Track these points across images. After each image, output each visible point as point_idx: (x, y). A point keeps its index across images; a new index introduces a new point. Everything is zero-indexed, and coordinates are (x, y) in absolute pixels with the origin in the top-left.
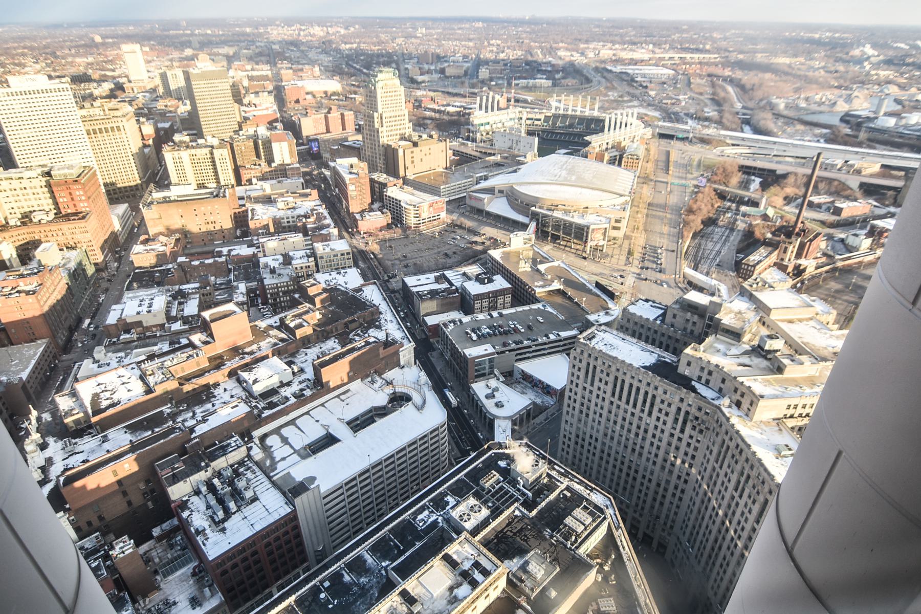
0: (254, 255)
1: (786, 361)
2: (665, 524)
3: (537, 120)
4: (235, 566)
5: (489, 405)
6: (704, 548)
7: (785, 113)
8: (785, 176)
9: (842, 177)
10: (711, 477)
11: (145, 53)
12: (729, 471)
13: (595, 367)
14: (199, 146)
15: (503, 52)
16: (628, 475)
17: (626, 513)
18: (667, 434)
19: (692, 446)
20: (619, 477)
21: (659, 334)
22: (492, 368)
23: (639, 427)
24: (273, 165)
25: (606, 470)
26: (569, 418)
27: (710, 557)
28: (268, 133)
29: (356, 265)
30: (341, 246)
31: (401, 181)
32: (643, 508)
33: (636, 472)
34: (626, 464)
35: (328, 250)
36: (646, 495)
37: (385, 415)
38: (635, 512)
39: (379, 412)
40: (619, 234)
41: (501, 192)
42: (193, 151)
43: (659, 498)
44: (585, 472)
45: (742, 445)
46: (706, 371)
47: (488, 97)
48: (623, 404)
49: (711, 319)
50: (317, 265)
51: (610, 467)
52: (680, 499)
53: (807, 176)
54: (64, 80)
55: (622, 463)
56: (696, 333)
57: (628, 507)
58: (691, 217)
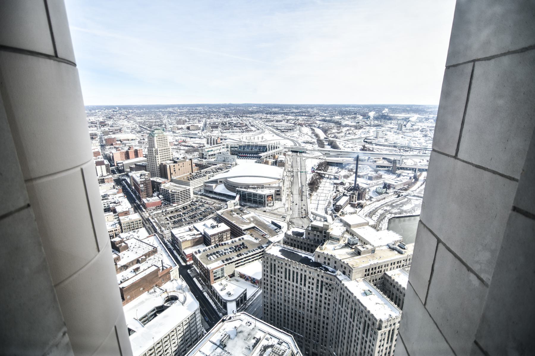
12: (346, 309)
16: (299, 320)
17: (302, 343)
18: (314, 294)
19: (327, 299)
23: (301, 293)
25: (288, 320)
29: (144, 226)
30: (135, 217)
33: (303, 318)
34: (298, 315)
35: (127, 220)
39: (161, 309)
41: (221, 182)
44: (278, 323)
50: (121, 228)
52: (327, 329)
55: (296, 315)
57: (302, 338)
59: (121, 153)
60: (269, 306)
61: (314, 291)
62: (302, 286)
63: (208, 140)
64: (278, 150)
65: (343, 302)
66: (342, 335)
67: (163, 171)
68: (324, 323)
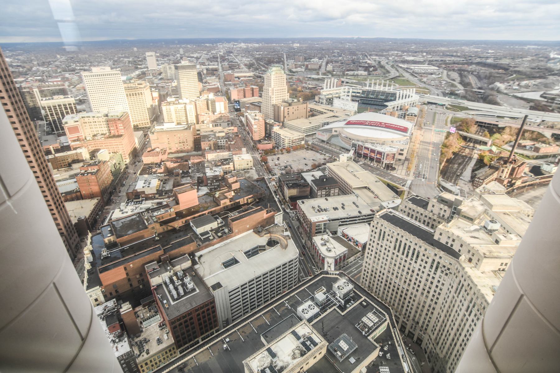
1: (501, 237)
2: (422, 327)
3: (358, 93)
4: (181, 324)
6: (446, 343)
7: (505, 91)
8: (503, 128)
9: (540, 130)
10: (451, 302)
11: (157, 57)
12: (463, 300)
13: (385, 232)
14: (179, 103)
15: (340, 56)
17: (399, 318)
20: (396, 297)
21: (424, 215)
22: (325, 228)
23: (409, 269)
24: (215, 114)
25: (388, 292)
26: (368, 260)
27: (449, 349)
28: (214, 98)
31: (281, 124)
32: (409, 316)
34: (400, 290)
36: (411, 309)
37: (264, 250)
38: (404, 318)
40: (403, 158)
42: (176, 106)
43: (419, 311)
44: (376, 292)
45: (471, 285)
46: (451, 239)
48: (400, 254)
49: (455, 209)
50: (234, 167)
51: (391, 291)
53: (518, 129)
54: (118, 69)
55: (398, 289)
56: (446, 217)
58: (446, 149)
60: (370, 273)
61: (426, 271)
62: (413, 262)
63: (327, 83)
65: (460, 291)
66: (450, 325)
67: (276, 113)
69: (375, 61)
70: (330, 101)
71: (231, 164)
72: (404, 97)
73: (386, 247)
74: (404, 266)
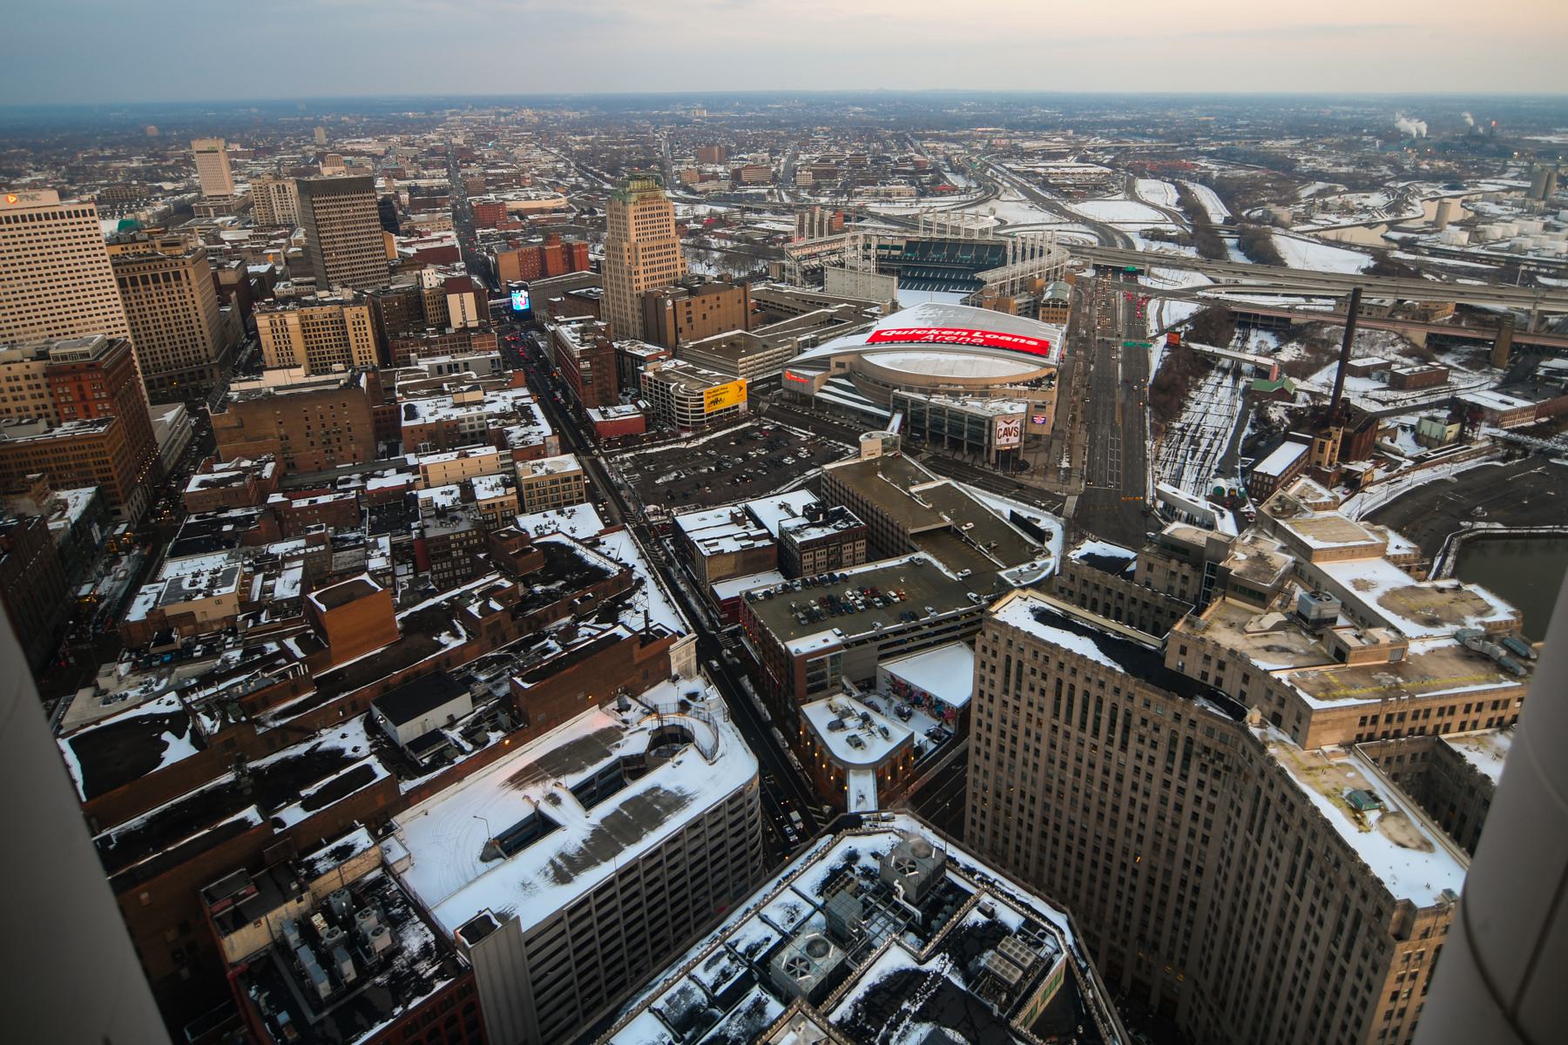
0: (410, 486)
5: (837, 744)
10: (1244, 860)
12: (1274, 847)
17: (1097, 940)
19: (1204, 803)
20: (1079, 871)
23: (1106, 772)
25: (1054, 856)
26: (980, 760)
29: (594, 499)
32: (1126, 929)
35: (540, 472)
36: (1131, 901)
38: (1113, 936)
42: (307, 310)
43: (1154, 905)
44: (1017, 863)
47: (812, 214)
48: (1074, 731)
49: (1213, 569)
52: (1193, 905)
55: (1083, 842)
56: (1190, 594)
59: (524, 257)
62: (1115, 749)
63: (802, 218)
64: (1045, 260)
65: (1263, 821)
66: (1251, 937)
68: (1183, 883)
69: (934, 154)
70: (815, 276)
71: (513, 489)
72: (1028, 254)
73: (1030, 710)
74: (1092, 766)
